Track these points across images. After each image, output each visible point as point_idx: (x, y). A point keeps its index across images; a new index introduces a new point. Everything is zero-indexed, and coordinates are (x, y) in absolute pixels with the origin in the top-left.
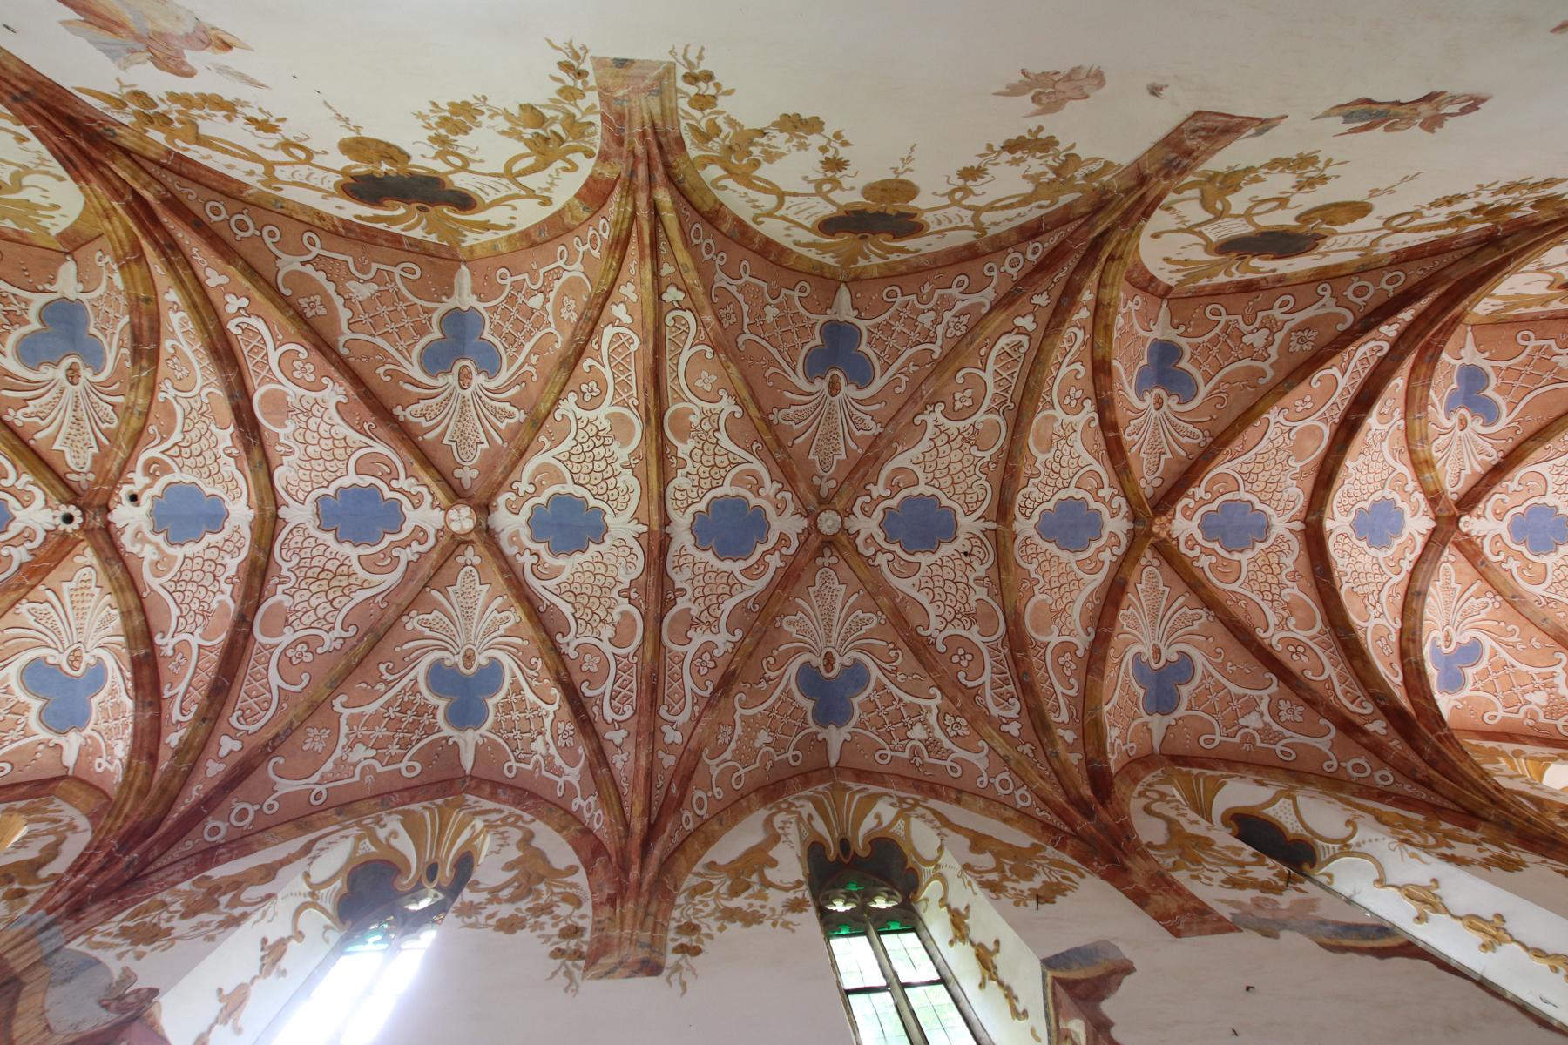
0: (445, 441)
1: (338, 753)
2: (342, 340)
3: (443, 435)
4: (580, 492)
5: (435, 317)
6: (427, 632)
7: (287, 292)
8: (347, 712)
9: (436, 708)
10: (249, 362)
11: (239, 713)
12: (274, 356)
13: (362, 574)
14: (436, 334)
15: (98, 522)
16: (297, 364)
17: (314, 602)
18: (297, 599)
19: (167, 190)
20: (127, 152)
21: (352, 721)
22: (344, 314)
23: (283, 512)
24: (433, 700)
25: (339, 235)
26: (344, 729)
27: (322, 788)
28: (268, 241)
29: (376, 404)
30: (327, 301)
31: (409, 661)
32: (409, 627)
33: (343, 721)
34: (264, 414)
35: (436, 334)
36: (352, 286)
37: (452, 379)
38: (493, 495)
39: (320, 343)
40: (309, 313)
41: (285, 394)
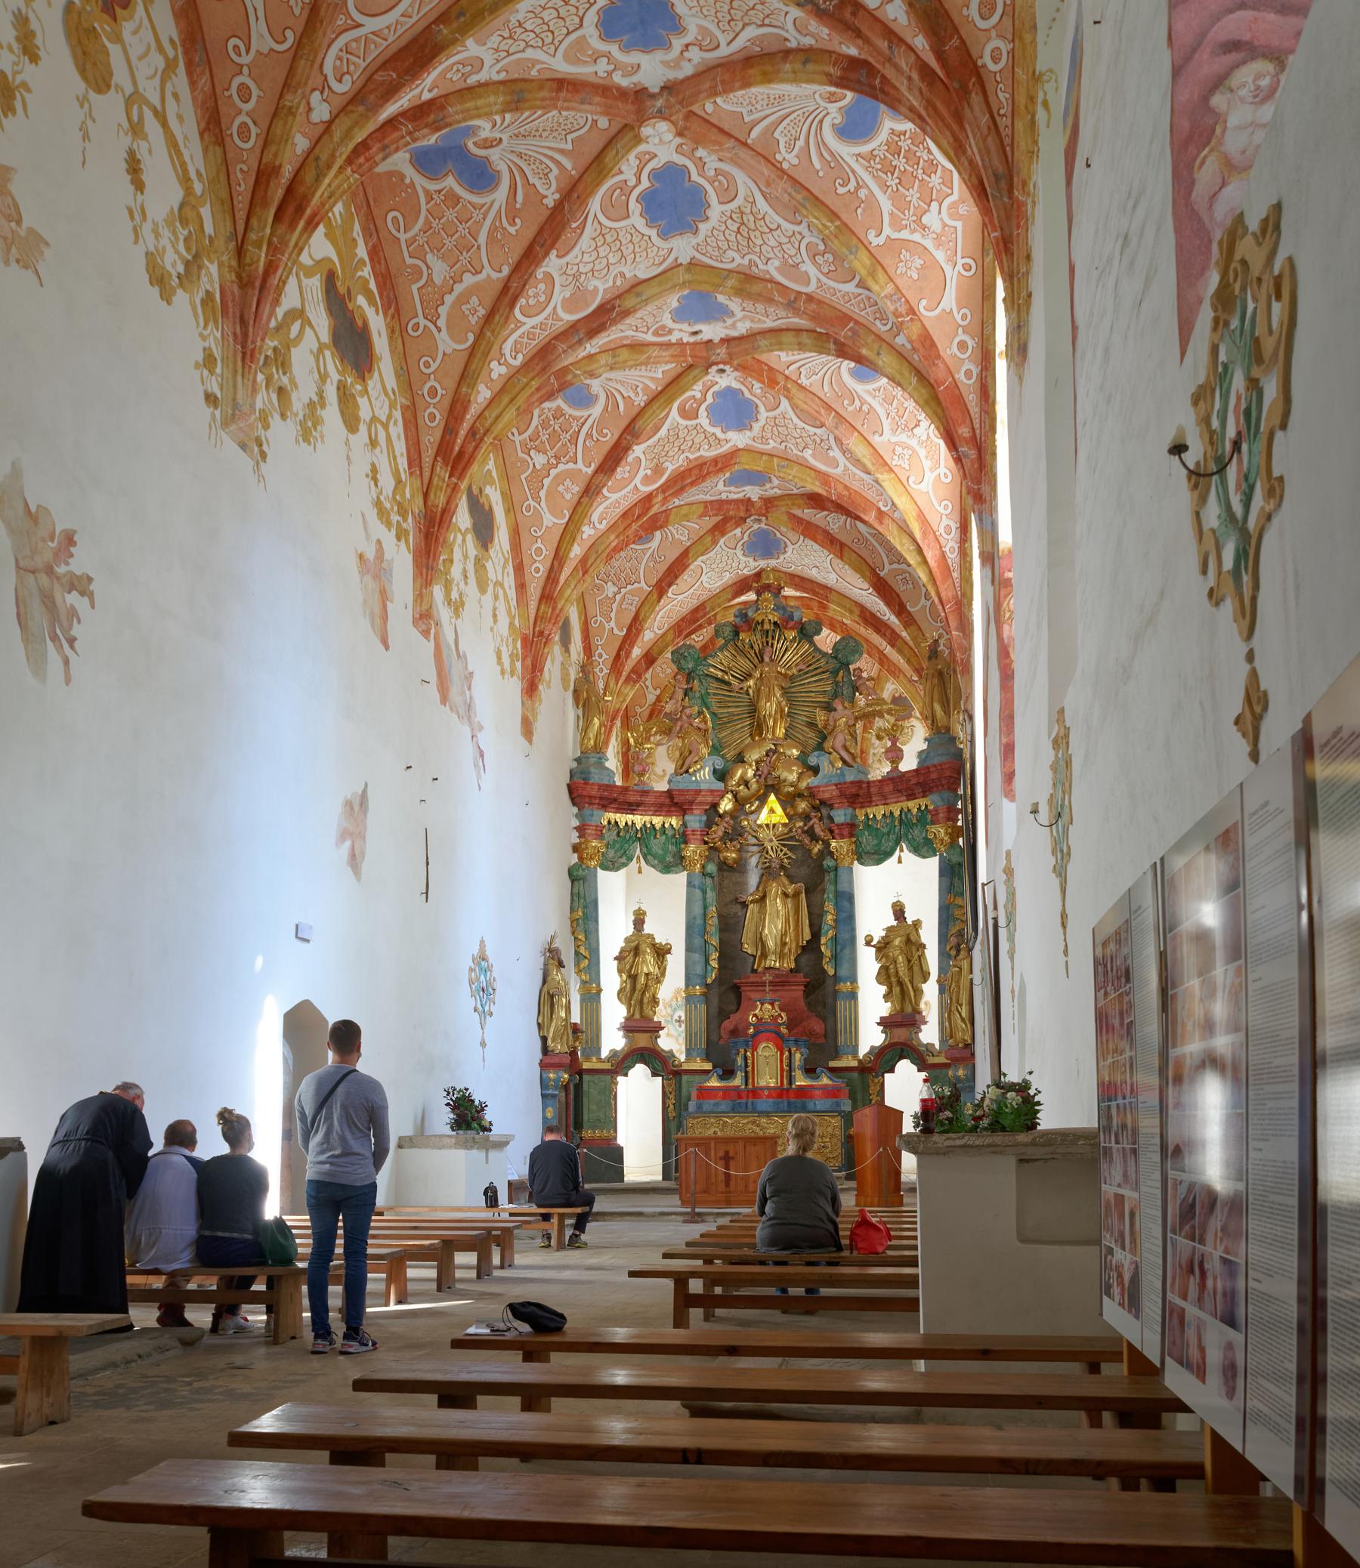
0: (569, 147)
1: (928, 243)
2: (495, 275)
3: (562, 151)
4: (591, 18)
5: (432, 186)
6: (801, 143)
7: (471, 337)
8: (887, 230)
9: (893, 132)
10: (542, 337)
11: (878, 322)
12: (531, 322)
13: (739, 201)
14: (450, 182)
15: (722, 351)
16: (532, 302)
17: (773, 243)
18: (771, 255)
19: (435, 459)
20: (426, 496)
21: (897, 226)
22: (469, 279)
23: (684, 260)
24: (883, 135)
25: (397, 310)
26: (905, 234)
27: (960, 262)
28: (434, 366)
29: (552, 229)
30: (463, 299)
31: (835, 164)
32: (796, 161)
33: (895, 235)
34: (588, 306)
35: (450, 182)
36: (438, 279)
37: (494, 155)
38: (622, 94)
39: (507, 300)
40: (482, 312)
41: (564, 300)
